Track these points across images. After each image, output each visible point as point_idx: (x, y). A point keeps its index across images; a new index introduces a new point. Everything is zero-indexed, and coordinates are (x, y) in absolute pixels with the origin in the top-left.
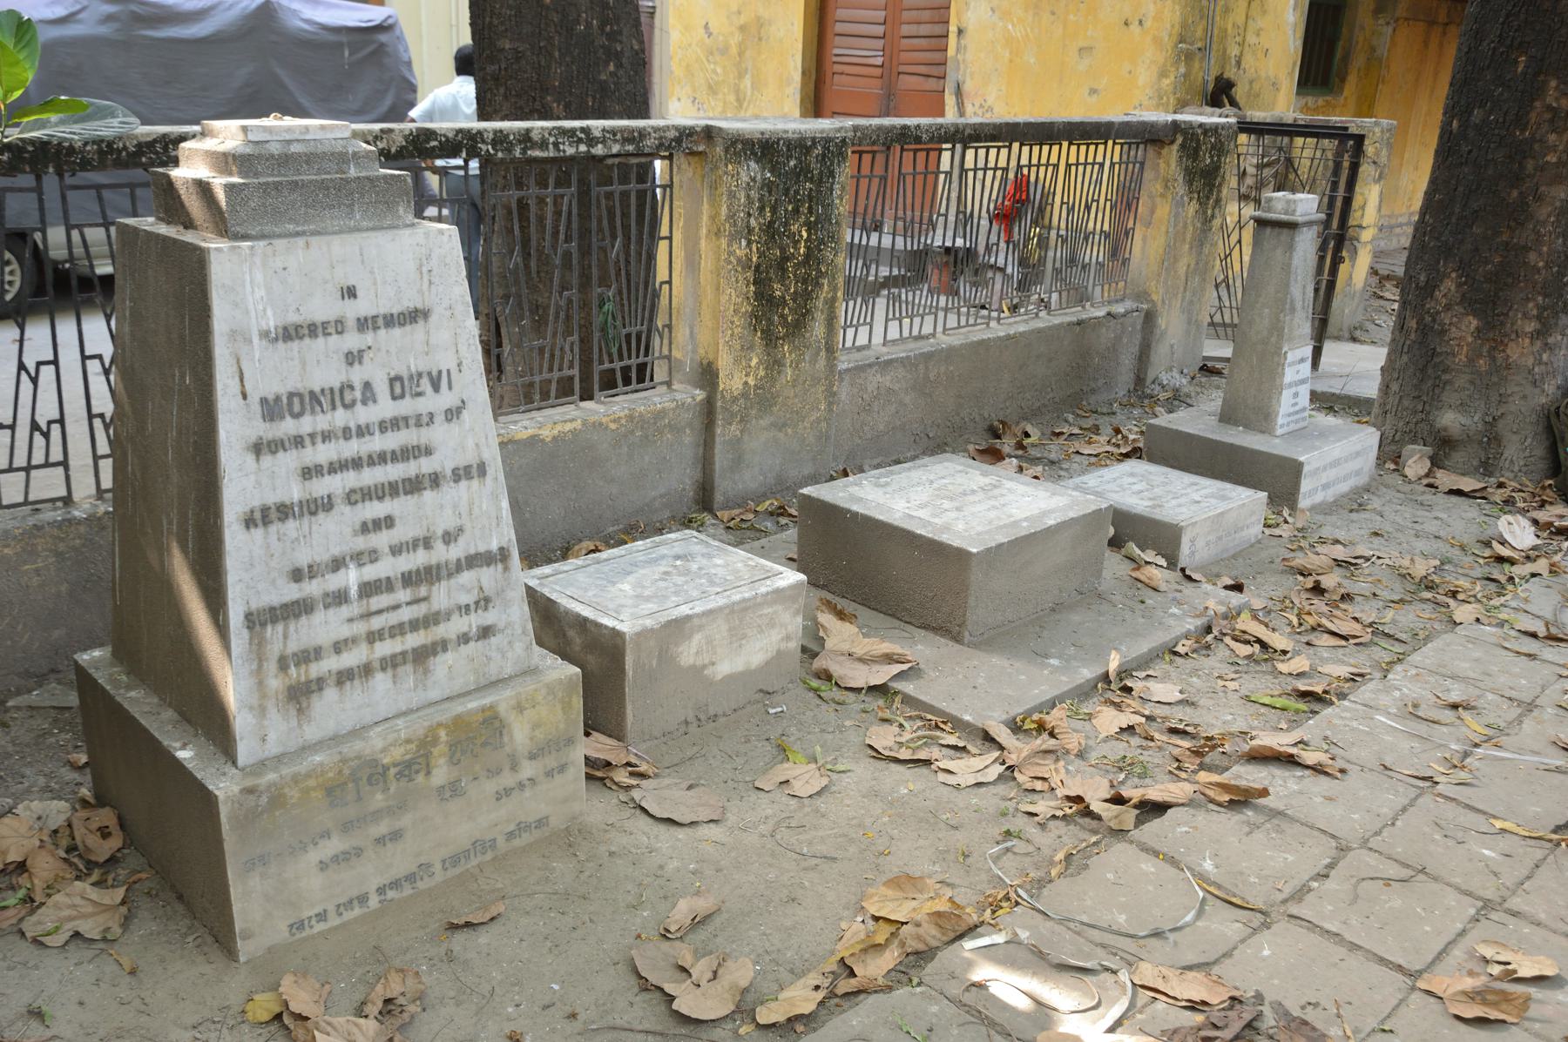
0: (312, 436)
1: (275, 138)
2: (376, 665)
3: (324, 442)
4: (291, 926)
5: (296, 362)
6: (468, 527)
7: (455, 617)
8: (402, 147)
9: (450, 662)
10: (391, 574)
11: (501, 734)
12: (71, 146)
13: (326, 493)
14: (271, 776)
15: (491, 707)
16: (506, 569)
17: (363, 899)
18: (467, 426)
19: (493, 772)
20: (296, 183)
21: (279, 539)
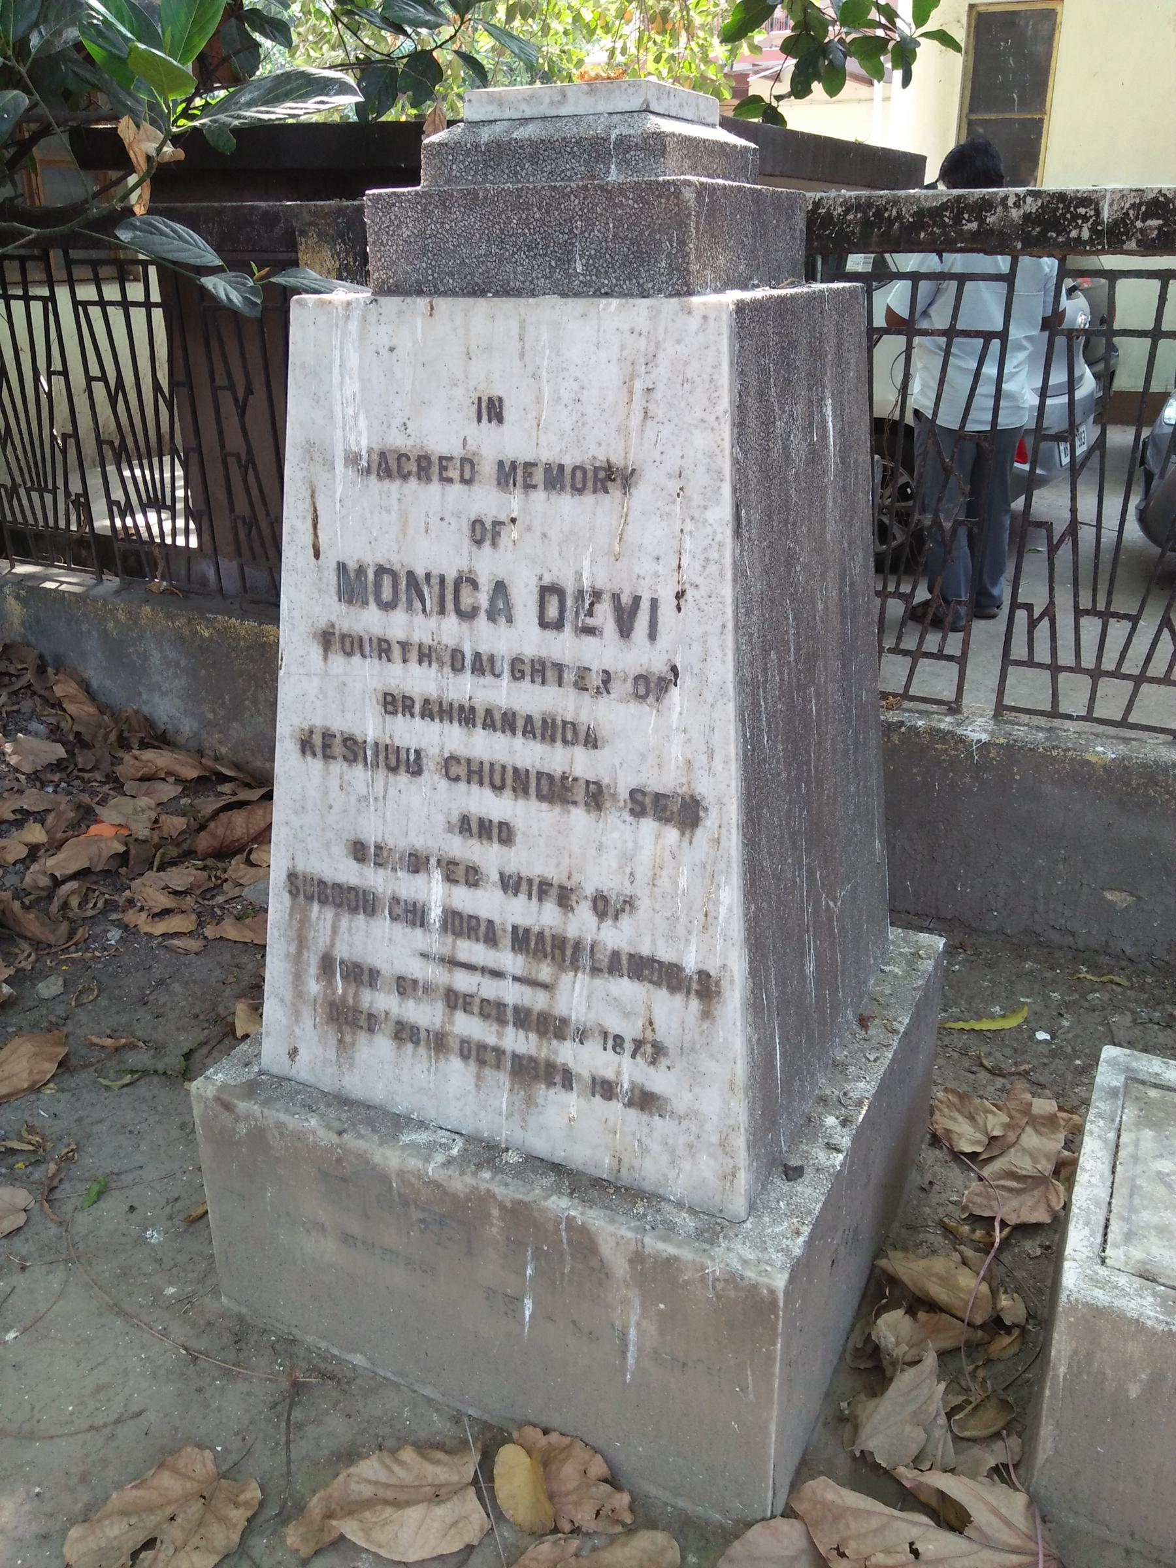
0: (405, 646)
1: (508, 114)
2: (455, 1044)
5: (394, 516)
6: (644, 904)
9: (573, 1113)
10: (497, 920)
13: (414, 746)
16: (706, 1014)
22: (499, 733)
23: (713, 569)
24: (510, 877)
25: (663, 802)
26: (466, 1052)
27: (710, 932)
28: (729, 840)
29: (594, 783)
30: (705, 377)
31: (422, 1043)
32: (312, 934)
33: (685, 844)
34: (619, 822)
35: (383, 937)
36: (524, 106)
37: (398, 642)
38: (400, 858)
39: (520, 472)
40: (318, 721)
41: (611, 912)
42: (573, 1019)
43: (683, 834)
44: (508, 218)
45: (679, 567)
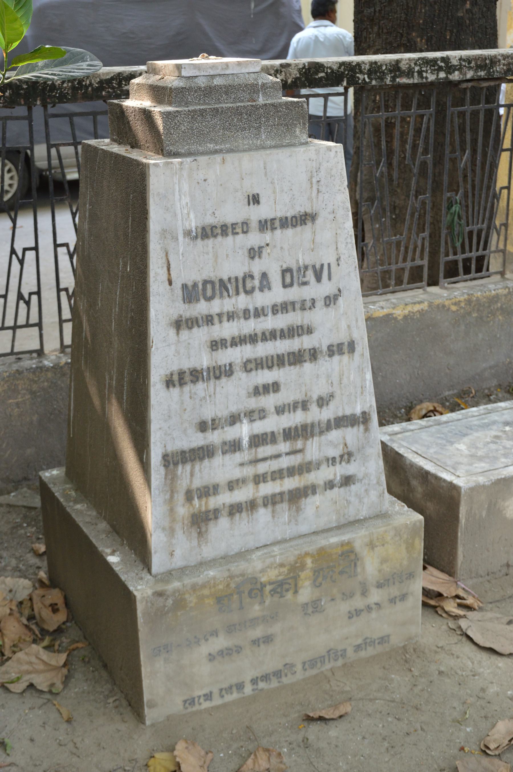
0: (220, 315)
2: (260, 501)
3: (228, 320)
4: (185, 702)
5: (211, 255)
7: (324, 467)
8: (296, 79)
9: (318, 503)
10: (275, 430)
12: (53, 84)
13: (228, 362)
14: (176, 584)
15: (349, 543)
16: (367, 430)
17: (240, 686)
18: (341, 311)
19: (347, 596)
20: (217, 110)
21: (191, 398)
22: (269, 342)
24: (280, 406)
25: (340, 347)
26: (266, 502)
27: (364, 394)
29: (312, 349)
30: (339, 174)
31: (244, 510)
32: (179, 482)
35: (219, 465)
36: (210, 70)
37: (217, 314)
38: (225, 421)
40: (175, 368)
41: (325, 403)
42: (314, 459)
43: (349, 357)
44: (232, 119)
45: (337, 248)
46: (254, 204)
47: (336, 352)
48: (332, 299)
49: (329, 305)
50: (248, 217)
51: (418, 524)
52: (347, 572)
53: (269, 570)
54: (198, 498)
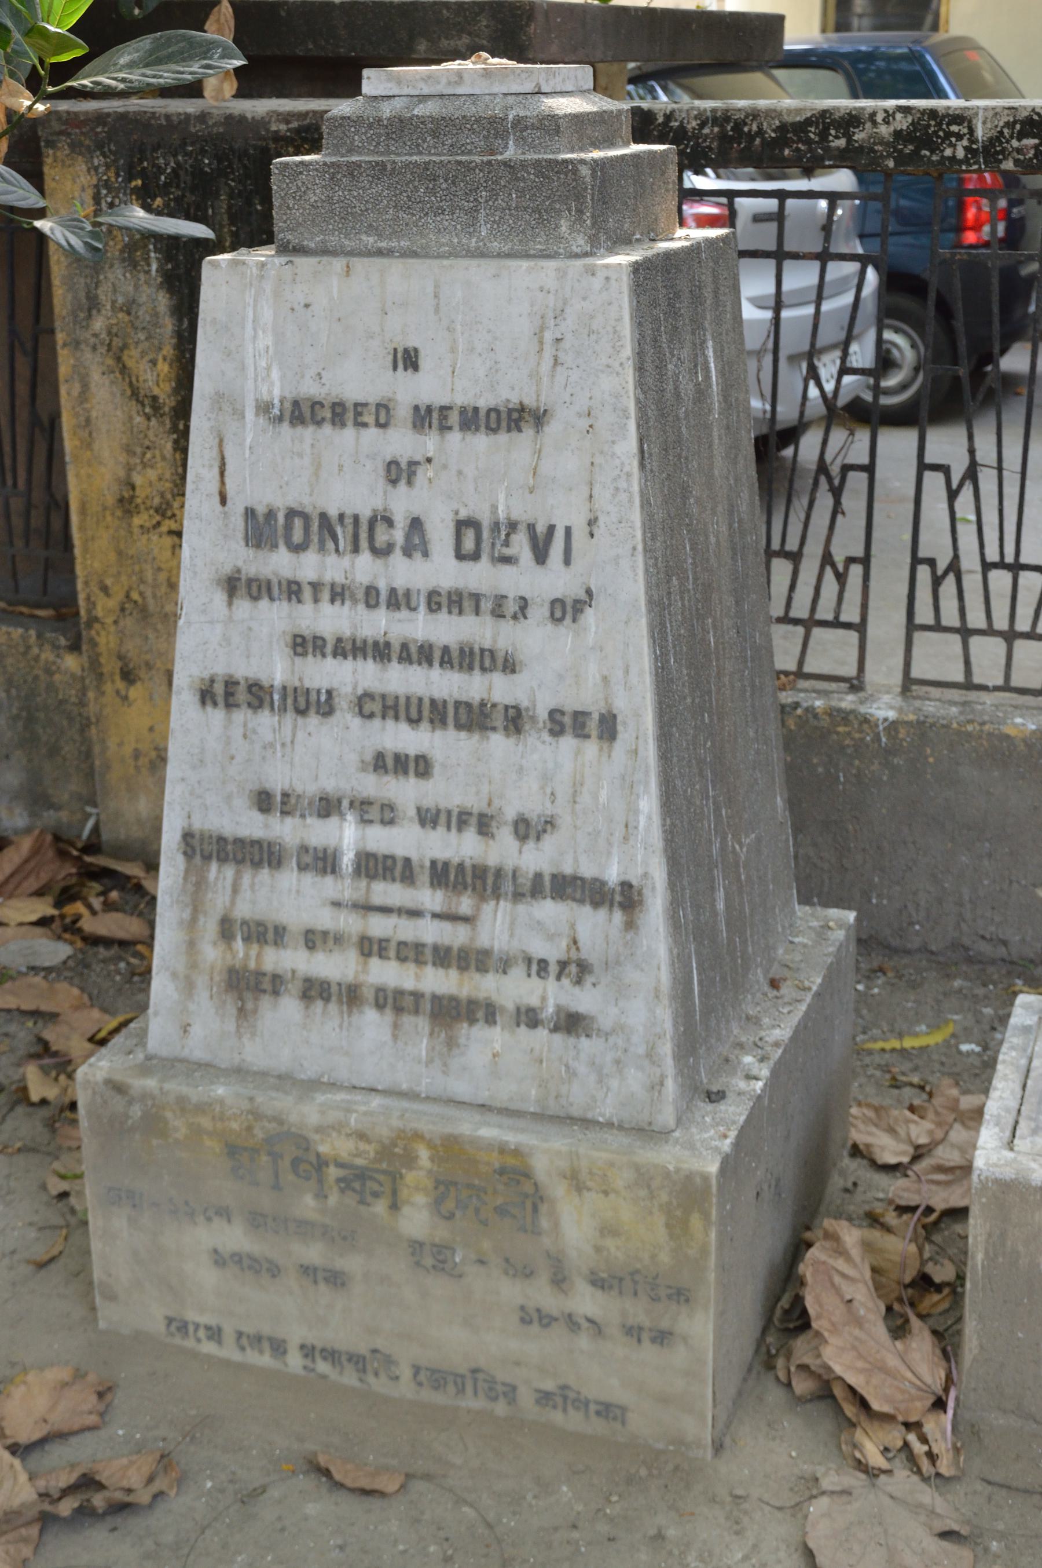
2: (369, 994)
3: (332, 601)
6: (565, 821)
7: (518, 972)
9: (498, 1047)
10: (414, 857)
11: (535, 1209)
12: (682, 127)
13: (325, 685)
15: (517, 1153)
16: (630, 925)
17: (279, 1348)
18: (591, 639)
20: (383, 165)
21: (245, 736)
22: (415, 666)
23: (623, 497)
24: (428, 810)
25: (580, 719)
26: (381, 1001)
27: (631, 842)
28: (646, 750)
29: (513, 707)
30: (609, 329)
31: (334, 998)
32: (210, 895)
33: (604, 758)
34: (538, 744)
35: (290, 890)
36: (422, 85)
38: (310, 804)
39: (435, 415)
40: (220, 669)
41: (533, 833)
42: (496, 948)
43: (601, 749)
45: (591, 496)
46: (406, 369)
47: (569, 729)
48: (569, 609)
49: (560, 620)
50: (391, 395)
51: (698, 1180)
52: (514, 1217)
53: (334, 1134)
54: (243, 939)
